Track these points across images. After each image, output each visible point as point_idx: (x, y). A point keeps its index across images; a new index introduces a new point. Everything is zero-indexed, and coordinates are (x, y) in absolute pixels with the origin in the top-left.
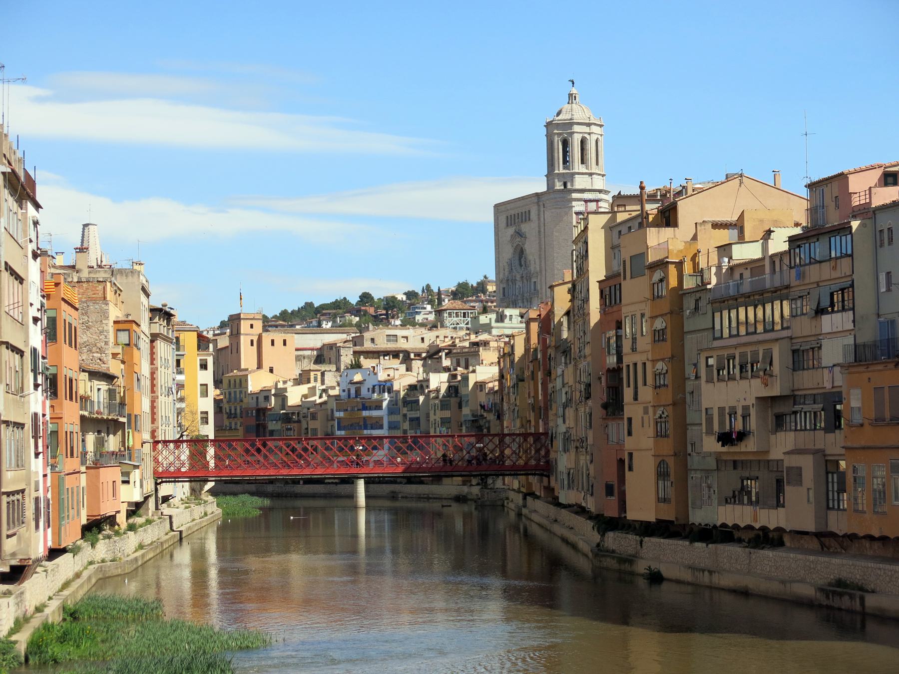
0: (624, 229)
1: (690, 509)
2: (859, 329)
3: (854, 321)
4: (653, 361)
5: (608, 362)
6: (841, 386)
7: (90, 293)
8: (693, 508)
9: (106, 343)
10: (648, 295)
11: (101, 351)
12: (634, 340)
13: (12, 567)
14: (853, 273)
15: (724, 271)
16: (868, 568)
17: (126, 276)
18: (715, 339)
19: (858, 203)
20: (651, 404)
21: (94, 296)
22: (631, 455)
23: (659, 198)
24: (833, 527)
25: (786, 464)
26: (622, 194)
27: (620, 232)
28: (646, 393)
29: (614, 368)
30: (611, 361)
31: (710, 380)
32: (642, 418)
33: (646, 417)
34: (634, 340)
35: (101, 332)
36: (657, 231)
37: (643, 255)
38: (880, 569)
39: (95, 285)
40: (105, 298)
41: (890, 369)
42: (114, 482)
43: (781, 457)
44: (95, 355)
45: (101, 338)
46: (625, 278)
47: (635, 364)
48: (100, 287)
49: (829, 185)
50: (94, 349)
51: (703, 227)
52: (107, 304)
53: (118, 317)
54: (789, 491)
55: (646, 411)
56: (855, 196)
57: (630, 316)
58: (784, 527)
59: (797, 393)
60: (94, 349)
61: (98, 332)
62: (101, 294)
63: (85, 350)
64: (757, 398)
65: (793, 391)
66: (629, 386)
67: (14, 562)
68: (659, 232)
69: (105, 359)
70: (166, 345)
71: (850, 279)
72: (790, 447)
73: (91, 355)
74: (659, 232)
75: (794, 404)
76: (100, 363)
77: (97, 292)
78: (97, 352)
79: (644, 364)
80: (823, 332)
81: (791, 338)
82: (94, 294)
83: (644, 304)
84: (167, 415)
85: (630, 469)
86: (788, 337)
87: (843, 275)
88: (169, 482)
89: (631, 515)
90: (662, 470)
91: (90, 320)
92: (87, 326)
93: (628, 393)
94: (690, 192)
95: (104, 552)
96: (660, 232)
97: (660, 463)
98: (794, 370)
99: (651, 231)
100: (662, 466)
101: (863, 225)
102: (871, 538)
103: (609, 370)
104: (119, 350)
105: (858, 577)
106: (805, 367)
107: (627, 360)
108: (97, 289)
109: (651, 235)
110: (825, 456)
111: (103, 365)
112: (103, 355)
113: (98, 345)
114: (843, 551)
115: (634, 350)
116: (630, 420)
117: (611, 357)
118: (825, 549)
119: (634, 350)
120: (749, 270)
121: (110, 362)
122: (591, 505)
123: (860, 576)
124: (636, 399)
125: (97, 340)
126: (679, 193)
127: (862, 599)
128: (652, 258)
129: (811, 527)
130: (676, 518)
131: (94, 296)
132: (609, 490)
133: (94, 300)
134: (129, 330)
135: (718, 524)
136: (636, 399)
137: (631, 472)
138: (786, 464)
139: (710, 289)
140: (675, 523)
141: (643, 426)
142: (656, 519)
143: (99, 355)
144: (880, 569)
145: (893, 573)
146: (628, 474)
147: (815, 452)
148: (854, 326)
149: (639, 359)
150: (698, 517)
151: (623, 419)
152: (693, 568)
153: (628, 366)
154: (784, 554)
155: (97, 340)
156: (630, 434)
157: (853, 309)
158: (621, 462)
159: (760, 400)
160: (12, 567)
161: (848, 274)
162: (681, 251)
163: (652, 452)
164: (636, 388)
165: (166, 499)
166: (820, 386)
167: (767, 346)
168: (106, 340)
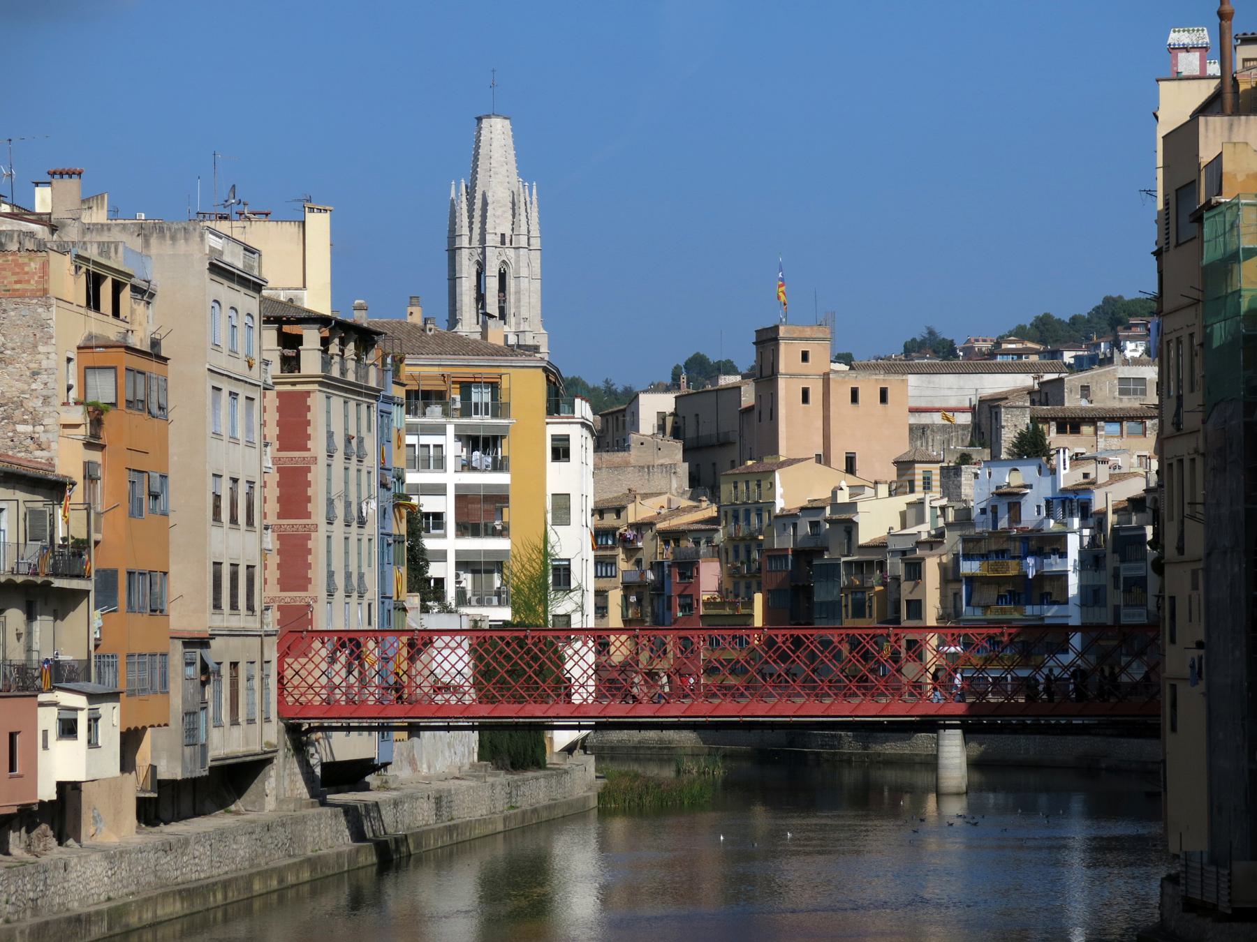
17: (173, 238)
21: (18, 286)
22: (1174, 687)
32: (1190, 597)
36: (1226, 125)
39: (21, 260)
40: (45, 292)
42: (12, 736)
44: (20, 428)
45: (34, 386)
47: (1181, 461)
57: (1174, 340)
61: (28, 374)
68: (1231, 126)
69: (43, 438)
73: (11, 427)
74: (1231, 126)
76: (32, 446)
77: (26, 277)
78: (25, 422)
82: (16, 282)
84: (353, 568)
88: (360, 729)
91: (10, 345)
99: (1211, 127)
108: (26, 269)
109: (1211, 134)
111: (38, 453)
112: (40, 429)
116: (1173, 599)
121: (54, 446)
124: (1181, 549)
125: (23, 392)
131: (18, 286)
134: (115, 368)
136: (1181, 549)
141: (1190, 621)
143: (29, 428)
155: (23, 392)
168: (45, 392)
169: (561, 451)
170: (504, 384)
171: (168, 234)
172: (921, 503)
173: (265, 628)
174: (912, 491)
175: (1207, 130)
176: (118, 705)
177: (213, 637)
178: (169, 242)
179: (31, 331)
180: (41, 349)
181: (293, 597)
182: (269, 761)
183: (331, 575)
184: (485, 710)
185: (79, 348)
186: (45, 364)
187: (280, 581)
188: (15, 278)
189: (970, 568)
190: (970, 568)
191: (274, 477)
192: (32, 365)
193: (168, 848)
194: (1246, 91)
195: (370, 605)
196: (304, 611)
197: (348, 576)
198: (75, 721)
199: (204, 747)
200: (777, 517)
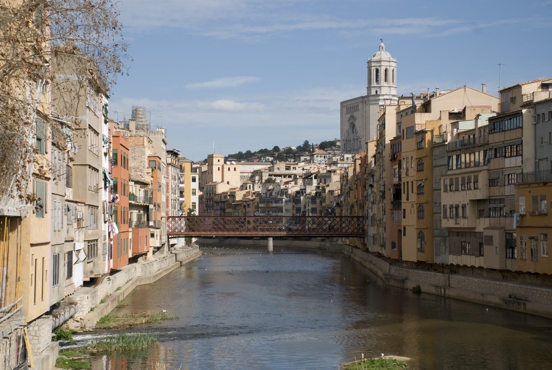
0: (404, 114)
1: (434, 256)
2: (525, 166)
3: (522, 162)
4: (417, 181)
5: (394, 181)
6: (514, 195)
7: (136, 142)
8: (436, 255)
9: (144, 167)
10: (415, 147)
12: (407, 170)
14: (522, 136)
15: (454, 135)
16: (528, 289)
17: (155, 134)
18: (449, 170)
19: (526, 100)
20: (416, 202)
22: (405, 228)
23: (422, 98)
24: (509, 267)
25: (485, 234)
26: (403, 96)
27: (402, 115)
28: (413, 197)
29: (397, 184)
30: (396, 181)
31: (445, 191)
32: (411, 209)
33: (413, 209)
34: (407, 170)
35: (141, 162)
37: (413, 127)
38: (534, 290)
40: (143, 145)
41: (541, 187)
43: (482, 230)
44: (138, 173)
46: (403, 139)
47: (408, 182)
48: (141, 139)
49: (511, 91)
50: (138, 170)
51: (444, 113)
52: (144, 148)
53: (150, 154)
54: (486, 248)
55: (413, 206)
56: (525, 96)
58: (483, 267)
59: (491, 198)
60: (138, 170)
62: (141, 143)
64: (470, 200)
65: (489, 197)
66: (404, 193)
68: (421, 116)
69: (143, 175)
70: (173, 168)
71: (520, 140)
72: (487, 225)
73: (136, 173)
75: (490, 204)
78: (139, 172)
79: (412, 182)
80: (505, 167)
81: (488, 170)
83: (413, 152)
85: (404, 235)
86: (487, 169)
87: (517, 138)
89: (404, 258)
90: (420, 236)
91: (136, 156)
92: (134, 159)
93: (404, 197)
94: (438, 95)
95: (140, 272)
97: (419, 233)
98: (490, 186)
100: (420, 234)
101: (529, 112)
102: (529, 273)
103: (394, 185)
104: (150, 170)
105: (522, 293)
106: (496, 185)
107: (403, 180)
110: (505, 230)
111: (142, 179)
112: (143, 173)
113: (140, 168)
114: (515, 280)
115: (407, 175)
116: (404, 210)
117: (396, 178)
118: (505, 278)
119: (407, 175)
120: (467, 135)
121: (145, 177)
122: (384, 252)
123: (524, 293)
124: (408, 200)
126: (432, 96)
127: (525, 304)
128: (418, 129)
129: (497, 266)
130: (427, 260)
132: (393, 245)
133: (138, 146)
134: (155, 161)
135: (449, 264)
136: (408, 200)
137: (404, 237)
138: (485, 234)
139: (447, 144)
140: (427, 263)
141: (411, 213)
142: (417, 260)
143: (140, 173)
144: (534, 290)
145: (542, 292)
146: (403, 237)
147: (500, 228)
148: (522, 164)
149: (410, 179)
150: (438, 260)
151: (401, 210)
152: (436, 287)
153: (404, 183)
154: (483, 280)
156: (404, 217)
157: (522, 155)
158: (400, 231)
159: (472, 201)
161: (519, 137)
163: (416, 227)
164: (408, 194)
165: (173, 245)
166: (503, 194)
167: (476, 174)
168: (144, 166)
169: (194, 180)
170: (183, 166)
171: (154, 133)
172: (249, 192)
174: (246, 189)
178: (154, 135)
179: (141, 153)
180: (143, 157)
182: (165, 244)
183: (172, 204)
184: (186, 233)
186: (144, 160)
188: (137, 142)
189: (261, 205)
190: (261, 205)
192: (141, 160)
194: (418, 109)
197: (174, 205)
198: (154, 234)
200: (217, 194)
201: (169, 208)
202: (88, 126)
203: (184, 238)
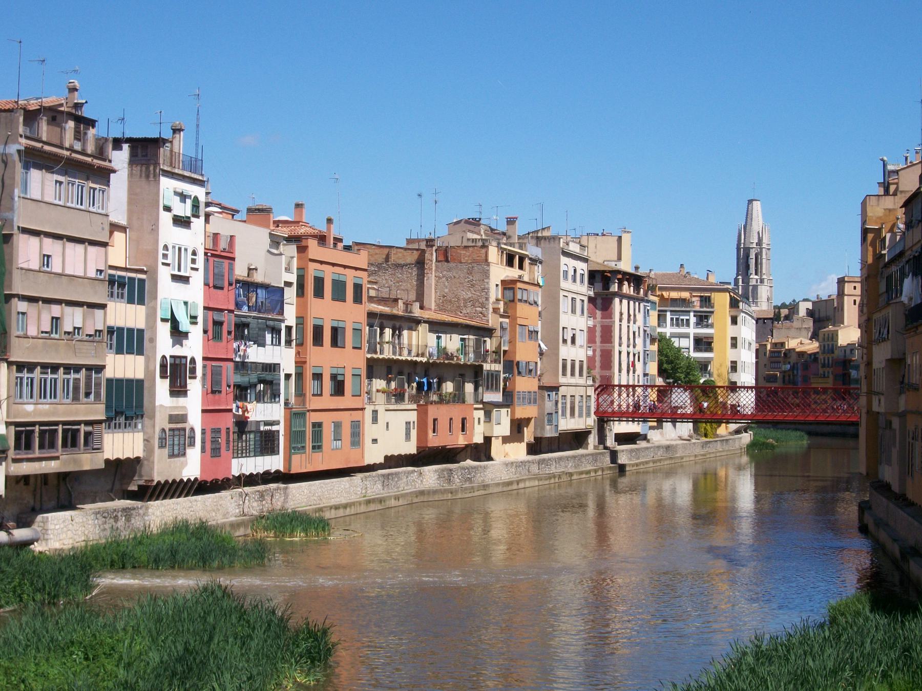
7: (475, 256)
9: (487, 299)
11: (483, 306)
13: (139, 486)
17: (549, 241)
21: (478, 258)
40: (486, 260)
44: (477, 309)
50: (477, 304)
63: (469, 304)
67: (142, 483)
78: (479, 307)
92: (471, 285)
96: (880, 201)
112: (484, 309)
113: (480, 300)
131: (478, 258)
133: (477, 262)
143: (481, 309)
160: (139, 486)
162: (880, 218)
173: (588, 383)
175: (870, 201)
176: (509, 410)
177: (561, 386)
181: (606, 373)
185: (502, 281)
186: (486, 286)
187: (601, 367)
191: (598, 329)
193: (540, 462)
195: (638, 376)
196: (610, 378)
199: (557, 426)
201: (612, 369)
202: (16, 228)
203: (691, 424)
